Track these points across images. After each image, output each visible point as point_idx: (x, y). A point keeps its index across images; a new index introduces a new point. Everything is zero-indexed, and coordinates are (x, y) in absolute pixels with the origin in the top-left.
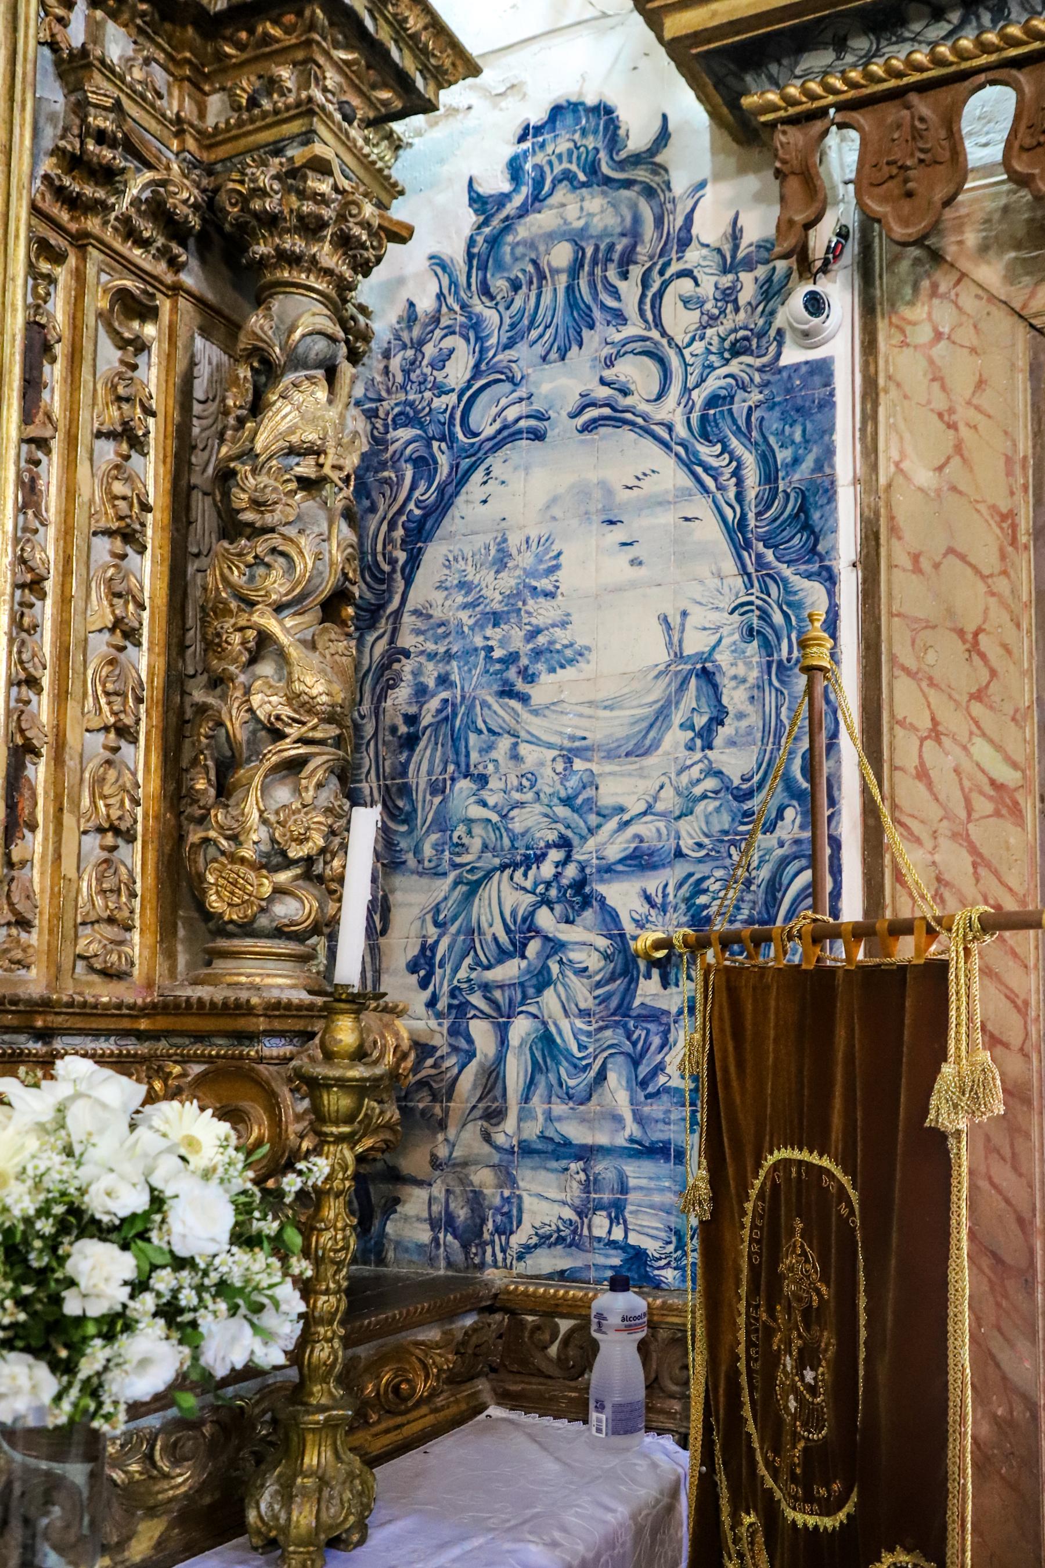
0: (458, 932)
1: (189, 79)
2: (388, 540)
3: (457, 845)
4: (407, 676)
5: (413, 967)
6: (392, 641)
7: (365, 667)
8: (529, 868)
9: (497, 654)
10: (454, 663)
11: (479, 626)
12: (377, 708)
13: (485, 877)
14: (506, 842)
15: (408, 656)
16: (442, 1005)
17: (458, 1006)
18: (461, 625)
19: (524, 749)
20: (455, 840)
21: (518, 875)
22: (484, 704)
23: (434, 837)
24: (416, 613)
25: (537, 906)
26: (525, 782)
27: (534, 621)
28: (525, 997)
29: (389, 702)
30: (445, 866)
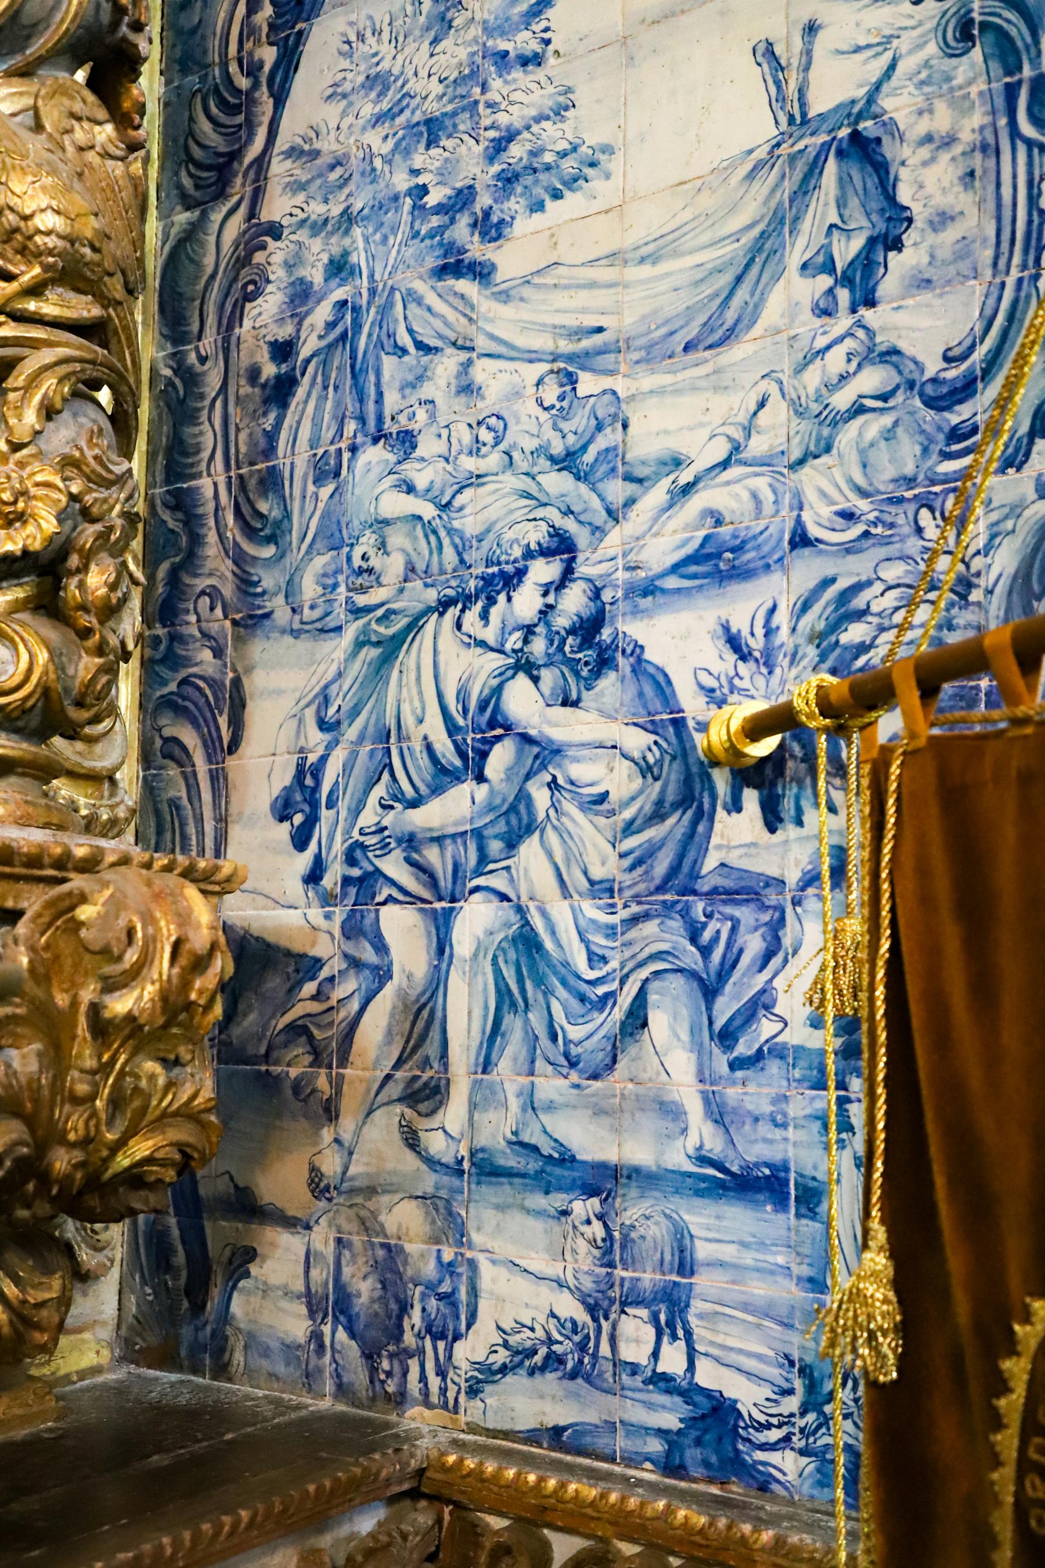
0: (361, 739)
2: (249, 31)
3: (360, 571)
4: (277, 274)
5: (283, 811)
6: (252, 214)
7: (209, 270)
8: (491, 601)
9: (432, 199)
10: (357, 232)
11: (404, 150)
12: (226, 340)
13: (409, 628)
14: (449, 555)
15: (277, 237)
16: (330, 880)
17: (361, 880)
18: (369, 156)
19: (482, 371)
20: (357, 562)
21: (471, 617)
22: (412, 297)
23: (320, 562)
24: (294, 153)
25: (504, 677)
26: (485, 436)
27: (503, 119)
28: (483, 858)
29: (247, 323)
30: (340, 614)
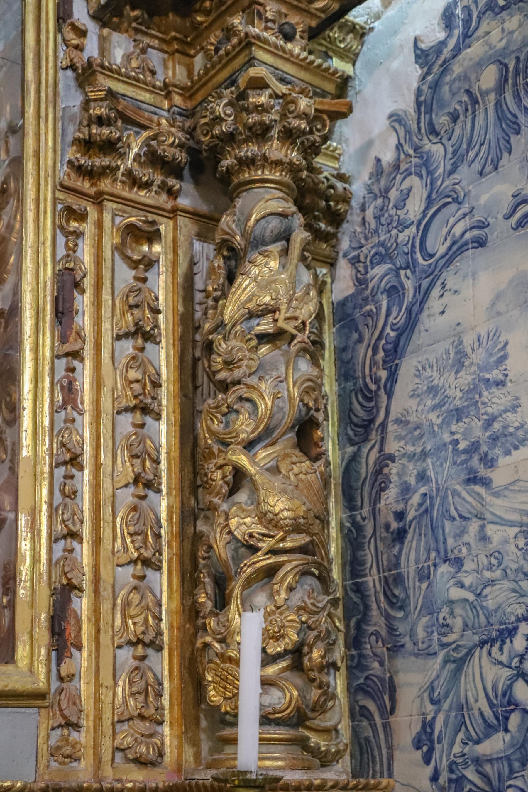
0: (450, 709)
1: (177, 51)
2: (374, 363)
3: (443, 626)
4: (394, 478)
5: (418, 745)
6: (381, 450)
7: (363, 476)
8: (503, 643)
9: (462, 446)
10: (429, 461)
11: (446, 423)
12: (374, 509)
13: (467, 654)
14: (483, 619)
15: (393, 461)
16: (443, 780)
17: (457, 781)
18: (432, 425)
19: (490, 530)
20: (441, 621)
21: (495, 650)
22: (455, 493)
23: (424, 620)
24: (398, 421)
25: (513, 680)
26: (494, 561)
27: (489, 410)
28: (512, 771)
29: (383, 502)
30: (435, 647)
